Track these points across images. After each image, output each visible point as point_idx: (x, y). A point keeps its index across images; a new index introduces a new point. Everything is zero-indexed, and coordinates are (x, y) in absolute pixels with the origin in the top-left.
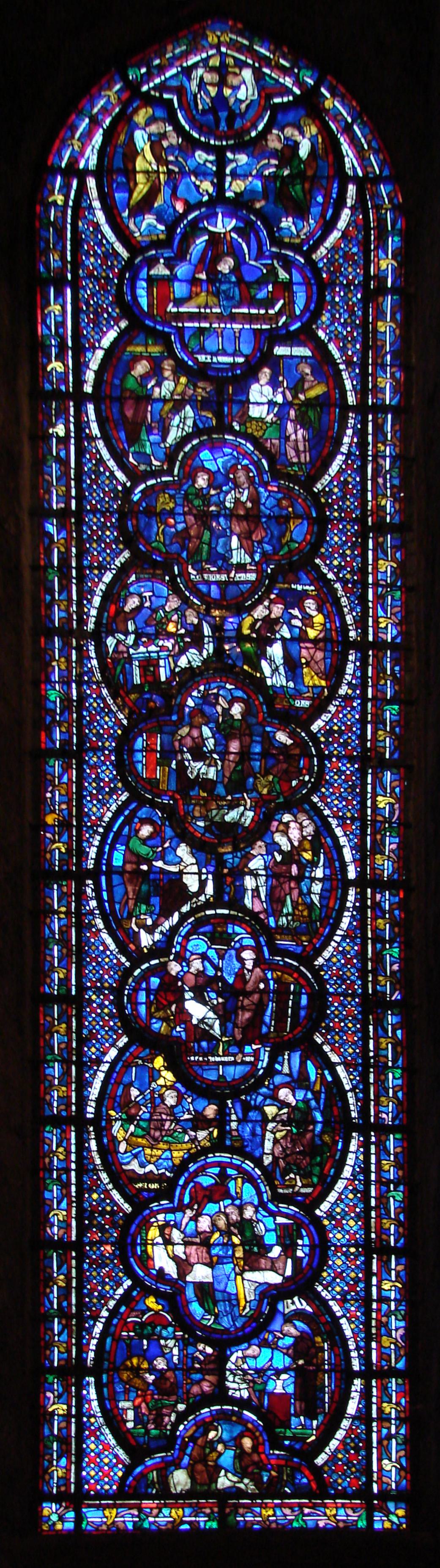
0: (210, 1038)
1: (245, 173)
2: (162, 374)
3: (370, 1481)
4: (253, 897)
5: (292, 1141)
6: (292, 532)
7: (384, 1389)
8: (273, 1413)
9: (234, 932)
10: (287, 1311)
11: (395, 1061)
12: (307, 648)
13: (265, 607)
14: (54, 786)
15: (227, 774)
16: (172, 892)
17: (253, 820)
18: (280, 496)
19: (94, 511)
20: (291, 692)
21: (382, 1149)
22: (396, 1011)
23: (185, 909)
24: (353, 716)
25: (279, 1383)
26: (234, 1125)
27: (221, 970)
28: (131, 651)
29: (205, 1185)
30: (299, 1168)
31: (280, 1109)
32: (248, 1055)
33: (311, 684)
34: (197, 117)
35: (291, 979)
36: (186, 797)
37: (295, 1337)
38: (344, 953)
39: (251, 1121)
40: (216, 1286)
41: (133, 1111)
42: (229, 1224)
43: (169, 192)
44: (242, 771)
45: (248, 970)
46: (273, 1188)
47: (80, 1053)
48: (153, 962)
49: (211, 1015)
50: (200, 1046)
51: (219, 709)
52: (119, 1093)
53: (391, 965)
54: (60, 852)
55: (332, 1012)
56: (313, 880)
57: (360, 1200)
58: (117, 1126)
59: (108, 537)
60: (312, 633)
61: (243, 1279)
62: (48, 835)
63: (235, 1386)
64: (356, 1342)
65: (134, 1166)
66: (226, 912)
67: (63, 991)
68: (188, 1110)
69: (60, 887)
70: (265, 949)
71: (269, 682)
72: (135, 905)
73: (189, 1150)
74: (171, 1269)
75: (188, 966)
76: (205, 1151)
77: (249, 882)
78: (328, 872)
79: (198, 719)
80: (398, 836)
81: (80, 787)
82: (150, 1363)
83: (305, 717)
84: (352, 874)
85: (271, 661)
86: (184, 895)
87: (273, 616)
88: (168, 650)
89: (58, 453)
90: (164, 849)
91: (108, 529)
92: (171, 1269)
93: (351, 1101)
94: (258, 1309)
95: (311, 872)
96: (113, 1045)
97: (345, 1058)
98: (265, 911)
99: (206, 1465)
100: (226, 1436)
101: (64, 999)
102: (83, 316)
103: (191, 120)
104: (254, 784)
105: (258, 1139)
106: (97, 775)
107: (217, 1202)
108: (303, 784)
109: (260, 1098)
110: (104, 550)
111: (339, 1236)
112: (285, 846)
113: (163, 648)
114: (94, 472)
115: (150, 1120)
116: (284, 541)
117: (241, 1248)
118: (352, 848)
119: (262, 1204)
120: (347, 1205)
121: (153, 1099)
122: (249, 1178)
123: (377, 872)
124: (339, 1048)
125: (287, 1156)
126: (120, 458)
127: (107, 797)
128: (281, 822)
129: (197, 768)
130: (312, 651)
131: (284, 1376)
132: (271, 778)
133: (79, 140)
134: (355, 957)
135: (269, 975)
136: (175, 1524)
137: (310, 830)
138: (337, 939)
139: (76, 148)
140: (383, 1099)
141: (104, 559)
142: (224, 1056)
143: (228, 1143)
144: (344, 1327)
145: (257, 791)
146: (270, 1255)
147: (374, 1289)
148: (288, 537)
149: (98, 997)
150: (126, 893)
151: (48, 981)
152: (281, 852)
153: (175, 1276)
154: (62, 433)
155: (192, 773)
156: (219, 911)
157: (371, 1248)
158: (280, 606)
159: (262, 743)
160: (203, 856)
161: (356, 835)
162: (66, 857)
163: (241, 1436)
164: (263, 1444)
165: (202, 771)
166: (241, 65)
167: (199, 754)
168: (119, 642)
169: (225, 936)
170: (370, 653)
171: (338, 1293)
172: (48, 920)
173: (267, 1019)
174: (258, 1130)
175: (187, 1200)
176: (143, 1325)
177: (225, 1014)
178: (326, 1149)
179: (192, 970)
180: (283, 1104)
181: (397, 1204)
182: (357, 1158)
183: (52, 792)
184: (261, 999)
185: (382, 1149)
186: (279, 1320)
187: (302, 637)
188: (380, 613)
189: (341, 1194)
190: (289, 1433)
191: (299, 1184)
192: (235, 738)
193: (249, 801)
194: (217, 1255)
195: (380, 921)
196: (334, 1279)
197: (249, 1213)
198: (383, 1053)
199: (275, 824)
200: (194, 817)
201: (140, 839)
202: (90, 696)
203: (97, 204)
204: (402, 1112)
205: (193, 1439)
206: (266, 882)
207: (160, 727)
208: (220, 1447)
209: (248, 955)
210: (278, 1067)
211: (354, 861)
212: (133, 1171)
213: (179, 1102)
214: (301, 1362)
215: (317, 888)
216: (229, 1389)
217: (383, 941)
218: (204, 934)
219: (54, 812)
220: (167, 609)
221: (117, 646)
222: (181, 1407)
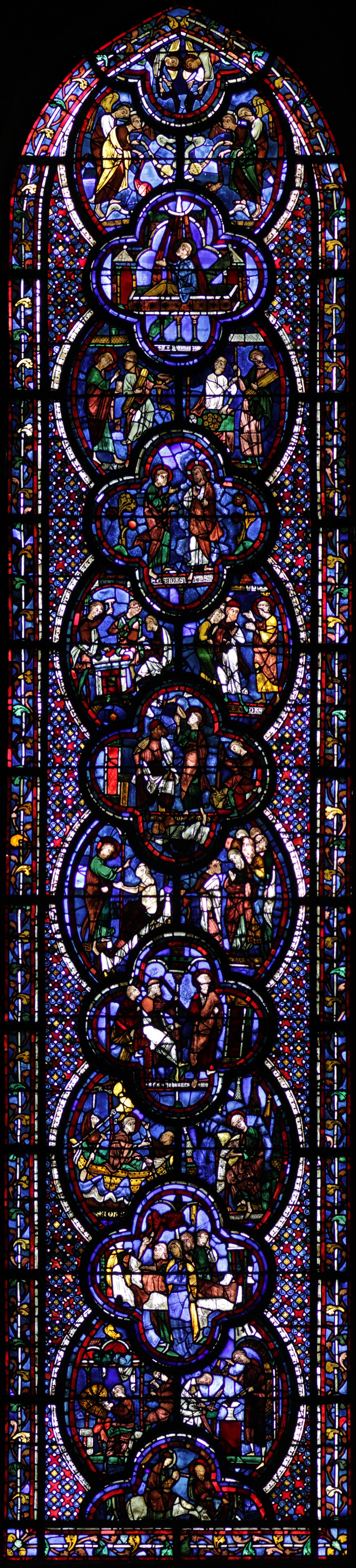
0: (167, 1063)
1: (205, 157)
2: (124, 366)
3: (314, 1508)
4: (209, 918)
5: (243, 1167)
6: (247, 530)
7: (328, 1415)
8: (225, 1439)
9: (190, 956)
10: (238, 1338)
11: (340, 1084)
12: (260, 653)
13: (221, 611)
14: (19, 806)
15: (185, 789)
16: (131, 913)
18: (235, 491)
19: (60, 515)
20: (246, 699)
21: (327, 1174)
22: (342, 1033)
23: (144, 931)
24: (304, 723)
25: (230, 1410)
26: (189, 1152)
27: (178, 994)
28: (95, 661)
29: (161, 1212)
30: (250, 1195)
31: (232, 1135)
32: (203, 1081)
33: (264, 690)
34: (160, 100)
35: (244, 1003)
36: (146, 814)
37: (246, 1365)
38: (294, 974)
39: (205, 1149)
40: (172, 1314)
41: (93, 1139)
42: (184, 1251)
43: (132, 175)
45: (204, 995)
46: (226, 1215)
47: (43, 1080)
48: (113, 987)
49: (168, 1040)
50: (157, 1072)
51: (177, 719)
52: (80, 1120)
53: (338, 985)
54: (24, 875)
55: (282, 1036)
56: (265, 899)
57: (306, 1225)
58: (78, 1154)
59: (73, 541)
60: (265, 637)
61: (197, 1307)
62: (13, 858)
63: (189, 1413)
64: (302, 1368)
65: (94, 1194)
66: (183, 934)
67: (26, 1018)
68: (146, 1137)
69: (24, 911)
70: (220, 972)
72: (96, 928)
73: (146, 1177)
74: (128, 1297)
75: (147, 990)
76: (161, 1180)
77: (205, 904)
78: (279, 889)
79: (157, 731)
80: (346, 849)
81: (45, 807)
82: (109, 1391)
83: (258, 725)
84: (302, 892)
85: (226, 668)
86: (143, 917)
87: (228, 620)
88: (129, 659)
89: (26, 454)
90: (124, 870)
91: (73, 533)
92: (128, 1297)
93: (299, 1125)
94: (210, 1336)
95: (263, 891)
96: (74, 1072)
97: (294, 1082)
98: (220, 933)
99: (162, 1493)
100: (180, 1463)
101: (28, 1027)
102: (51, 309)
103: (154, 103)
104: (210, 798)
105: (212, 1166)
106: (61, 794)
107: (172, 1229)
108: (256, 796)
109: (214, 1125)
110: (69, 556)
111: (287, 1262)
113: (123, 657)
114: (60, 473)
115: (109, 1148)
116: (239, 540)
117: (194, 1276)
118: (302, 864)
119: (215, 1231)
120: (294, 1230)
121: (112, 1126)
122: (202, 1205)
123: (327, 888)
124: (288, 1072)
125: (239, 1182)
126: (83, 456)
127: (70, 815)
128: (235, 839)
129: (156, 782)
130: (264, 656)
131: (235, 1404)
132: (226, 791)
133: (50, 128)
134: (304, 978)
135: (223, 1000)
136: (133, 1551)
137: (262, 845)
138: (288, 960)
139: (48, 135)
140: (329, 1122)
141: (69, 565)
142: (180, 1082)
143: (183, 1170)
144: (291, 1353)
145: (213, 805)
146: (222, 1283)
147: (319, 1314)
148: (242, 537)
149: (60, 1023)
150: (88, 915)
151: (12, 1007)
152: (235, 870)
153: (132, 1304)
154: (29, 433)
155: (151, 787)
156: (176, 934)
157: (317, 1273)
158: (235, 609)
159: (217, 755)
160: (160, 876)
161: (306, 850)
162: (30, 880)
163: (195, 1463)
164: (215, 1471)
165: (161, 785)
166: (201, 49)
167: (158, 767)
168: (82, 652)
169: (182, 959)
170: (320, 656)
171: (286, 1319)
172: (12, 945)
173: (221, 1044)
174: (212, 1157)
175: (144, 1227)
176: (102, 1353)
177: (182, 1040)
178: (275, 1174)
179: (150, 994)
180: (235, 1130)
181: (341, 1228)
182: (304, 1183)
183: (18, 812)
184: (215, 1024)
185: (327, 1174)
186: (231, 1347)
187: (255, 642)
188: (329, 612)
189: (289, 1219)
190: (239, 1461)
191: (250, 1210)
192: (192, 750)
194: (172, 1283)
195: (328, 939)
196: (282, 1305)
197: (203, 1239)
198: (330, 1075)
199: (230, 840)
200: (153, 835)
201: (101, 859)
202: (54, 709)
203: (66, 192)
204: (346, 1134)
205: (149, 1465)
206: (221, 903)
207: (122, 739)
208: (175, 1475)
209: (203, 979)
210: (231, 1093)
211: (305, 877)
212: (93, 1199)
213: (137, 1130)
214: (251, 1389)
215: (269, 907)
216: (184, 1416)
217: (331, 961)
218: (162, 958)
219: (18, 833)
220: (129, 616)
221: (80, 656)
222: (138, 1434)
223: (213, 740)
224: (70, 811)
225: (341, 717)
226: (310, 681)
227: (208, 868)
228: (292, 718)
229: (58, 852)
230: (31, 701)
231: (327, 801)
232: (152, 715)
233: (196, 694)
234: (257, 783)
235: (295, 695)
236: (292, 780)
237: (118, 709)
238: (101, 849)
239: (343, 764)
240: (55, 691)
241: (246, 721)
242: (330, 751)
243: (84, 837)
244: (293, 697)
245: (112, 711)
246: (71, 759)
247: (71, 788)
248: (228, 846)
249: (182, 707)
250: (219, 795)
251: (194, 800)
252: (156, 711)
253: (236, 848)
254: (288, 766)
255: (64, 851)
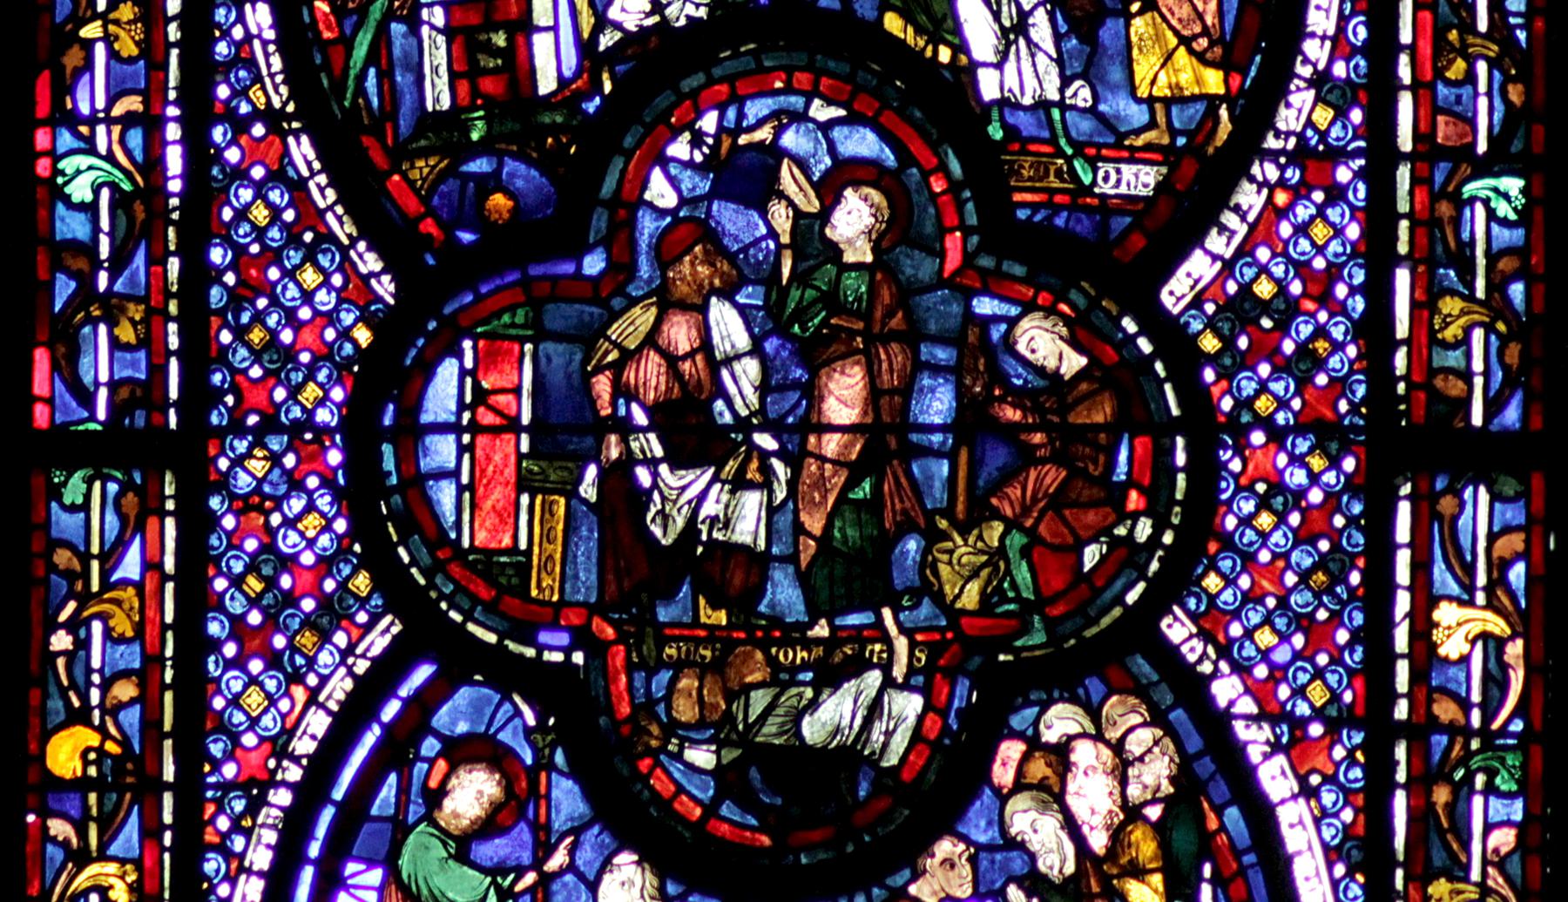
14: (85, 598)
17: (917, 736)
20: (1083, 126)
24: (1339, 232)
33: (1161, 90)
44: (874, 505)
51: (781, 217)
71: (989, 86)
79: (692, 269)
81: (197, 601)
83: (1138, 242)
104: (927, 564)
108: (1127, 556)
112: (1054, 855)
118: (1332, 854)
127: (307, 640)
128: (1034, 743)
129: (683, 496)
137: (1155, 773)
145: (938, 598)
155: (664, 516)
159: (954, 372)
161: (1348, 793)
165: (710, 508)
167: (692, 430)
193: (901, 644)
199: (1012, 750)
200: (671, 727)
202: (239, 174)
219: (80, 717)
223: (940, 308)
224: (308, 622)
225: (1503, 209)
226: (1366, 50)
227: (917, 875)
228: (1283, 213)
229: (253, 808)
230: (136, 138)
231: (1443, 578)
232: (669, 200)
233: (866, 105)
234: (1134, 500)
235: (1298, 110)
236: (1284, 486)
237: (520, 173)
238: (442, 792)
239: (1511, 415)
240: (241, 93)
241: (1083, 226)
242: (1454, 358)
243: (370, 738)
244: (1288, 119)
245: (491, 183)
246: (311, 392)
247: (312, 523)
248: (1003, 775)
249: (802, 164)
250: (964, 551)
251: (853, 573)
252: (688, 180)
253: (1041, 786)
254: (1267, 423)
255: (283, 797)
